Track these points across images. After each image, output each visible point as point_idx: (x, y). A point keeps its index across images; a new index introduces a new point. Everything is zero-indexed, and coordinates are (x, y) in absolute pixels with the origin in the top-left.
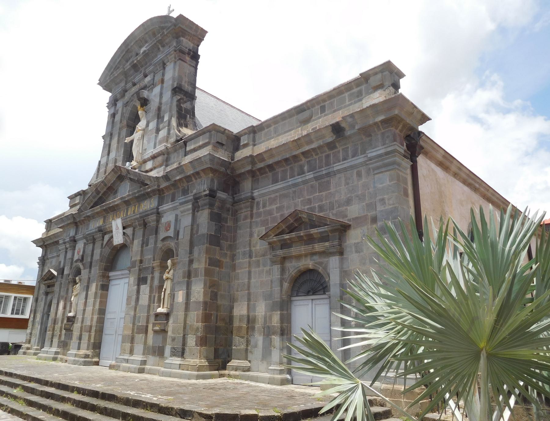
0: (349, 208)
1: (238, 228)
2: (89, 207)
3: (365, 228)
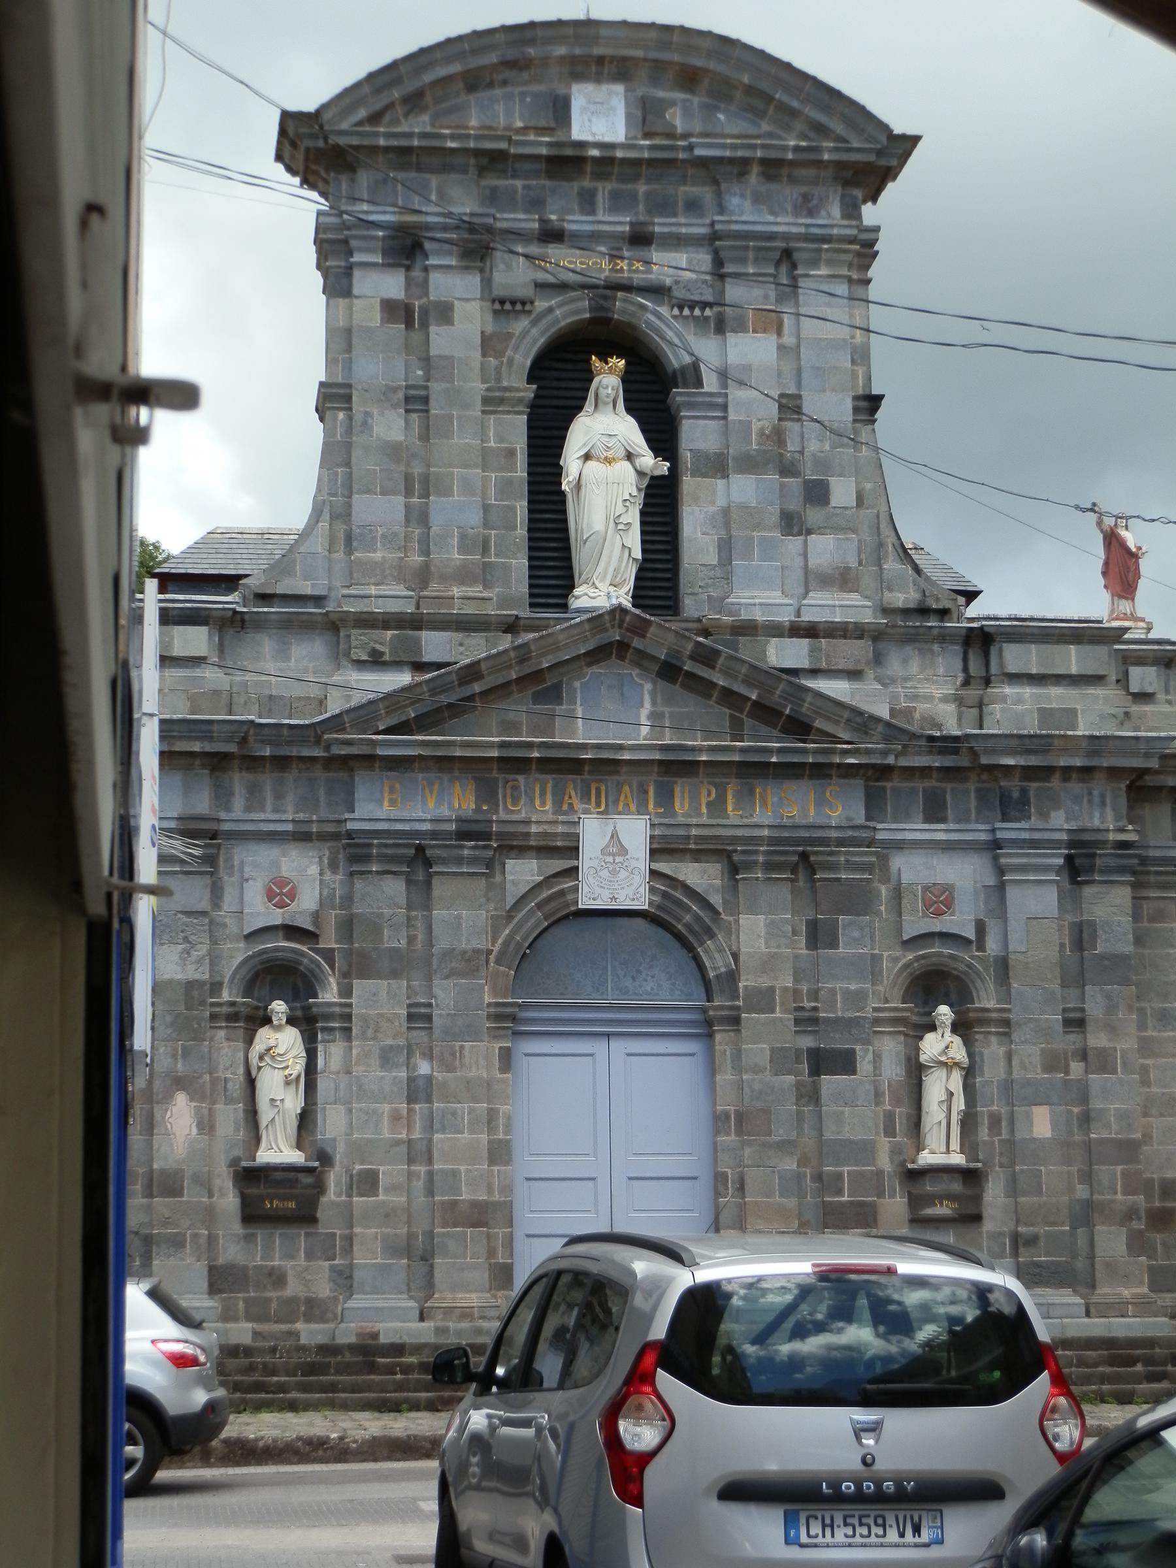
2: (392, 721)
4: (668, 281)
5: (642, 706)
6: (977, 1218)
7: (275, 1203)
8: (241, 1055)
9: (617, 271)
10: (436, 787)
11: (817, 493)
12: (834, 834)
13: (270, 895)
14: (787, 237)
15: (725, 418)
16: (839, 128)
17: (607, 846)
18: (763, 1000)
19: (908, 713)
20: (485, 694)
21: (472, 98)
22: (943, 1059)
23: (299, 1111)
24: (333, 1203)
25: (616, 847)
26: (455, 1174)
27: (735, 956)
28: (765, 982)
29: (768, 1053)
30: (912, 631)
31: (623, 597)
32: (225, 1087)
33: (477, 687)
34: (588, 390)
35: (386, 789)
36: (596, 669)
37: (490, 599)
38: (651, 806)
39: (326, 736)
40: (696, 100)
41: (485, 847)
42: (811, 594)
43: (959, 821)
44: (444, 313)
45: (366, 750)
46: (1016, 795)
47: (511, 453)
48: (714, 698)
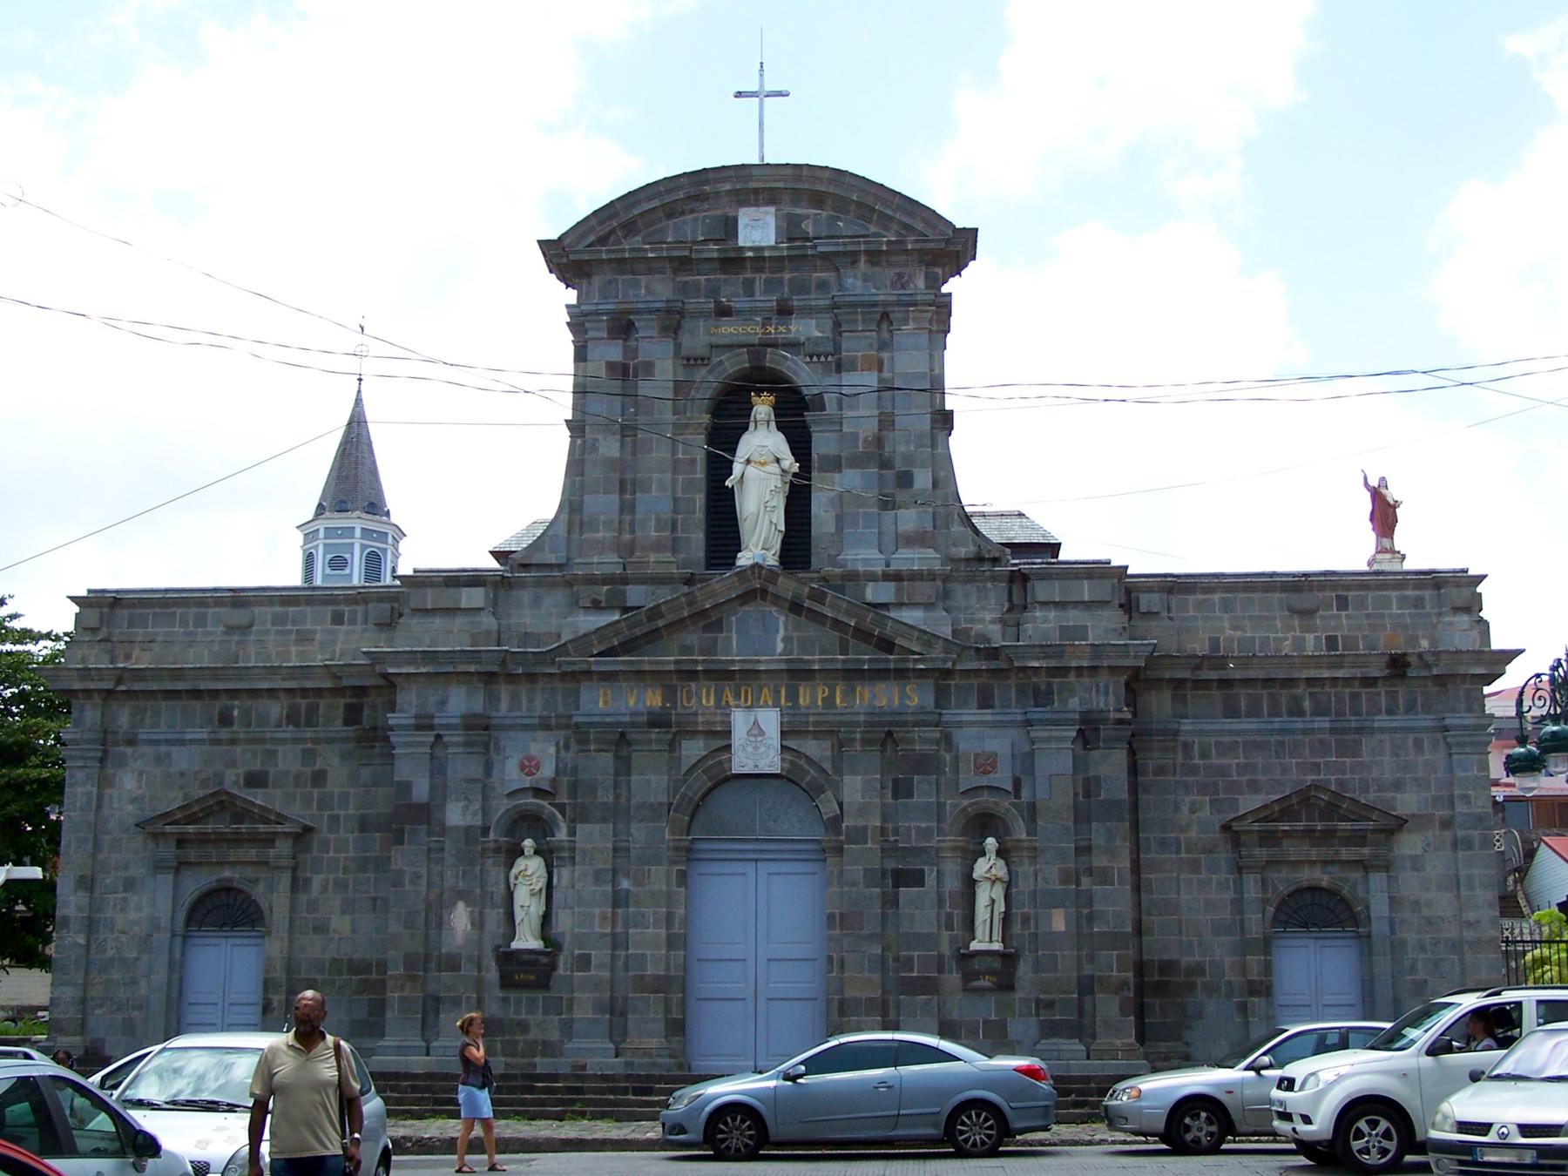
0: (1399, 796)
1: (1140, 789)
2: (603, 648)
4: (802, 339)
5: (778, 632)
6: (1011, 988)
7: (522, 976)
8: (502, 876)
9: (767, 334)
10: (635, 692)
11: (905, 480)
12: (910, 718)
13: (522, 767)
14: (886, 304)
15: (841, 431)
16: (920, 226)
17: (751, 730)
18: (859, 835)
19: (967, 631)
20: (668, 626)
21: (671, 222)
22: (988, 875)
23: (541, 913)
24: (561, 976)
26: (643, 955)
27: (841, 805)
29: (862, 872)
31: (772, 560)
33: (661, 623)
34: (750, 415)
35: (601, 693)
36: (746, 608)
38: (783, 702)
39: (557, 659)
40: (825, 214)
41: (666, 732)
42: (899, 551)
43: (1003, 707)
44: (649, 368)
45: (584, 667)
46: (1043, 687)
47: (693, 461)
48: (828, 625)
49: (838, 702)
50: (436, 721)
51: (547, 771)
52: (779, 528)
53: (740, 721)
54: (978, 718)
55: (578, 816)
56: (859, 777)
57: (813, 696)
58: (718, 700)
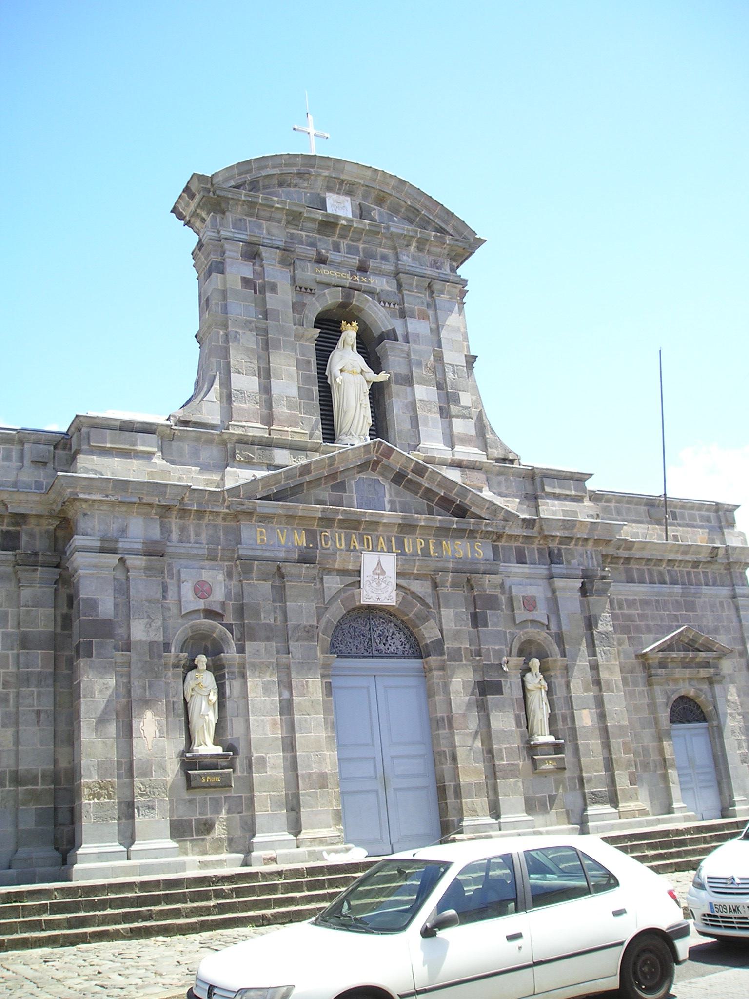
3: (735, 660)
7: (208, 778)
9: (354, 281)
17: (375, 569)
25: (380, 570)
28: (456, 645)
30: (502, 469)
32: (173, 708)
33: (308, 478)
37: (307, 434)
44: (274, 288)
46: (556, 551)
48: (419, 495)
49: (432, 553)
50: (120, 545)
51: (218, 595)
52: (368, 422)
53: (369, 561)
54: (521, 570)
55: (245, 635)
56: (452, 610)
57: (415, 546)
58: (348, 544)
